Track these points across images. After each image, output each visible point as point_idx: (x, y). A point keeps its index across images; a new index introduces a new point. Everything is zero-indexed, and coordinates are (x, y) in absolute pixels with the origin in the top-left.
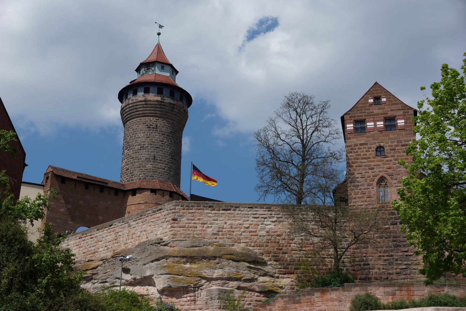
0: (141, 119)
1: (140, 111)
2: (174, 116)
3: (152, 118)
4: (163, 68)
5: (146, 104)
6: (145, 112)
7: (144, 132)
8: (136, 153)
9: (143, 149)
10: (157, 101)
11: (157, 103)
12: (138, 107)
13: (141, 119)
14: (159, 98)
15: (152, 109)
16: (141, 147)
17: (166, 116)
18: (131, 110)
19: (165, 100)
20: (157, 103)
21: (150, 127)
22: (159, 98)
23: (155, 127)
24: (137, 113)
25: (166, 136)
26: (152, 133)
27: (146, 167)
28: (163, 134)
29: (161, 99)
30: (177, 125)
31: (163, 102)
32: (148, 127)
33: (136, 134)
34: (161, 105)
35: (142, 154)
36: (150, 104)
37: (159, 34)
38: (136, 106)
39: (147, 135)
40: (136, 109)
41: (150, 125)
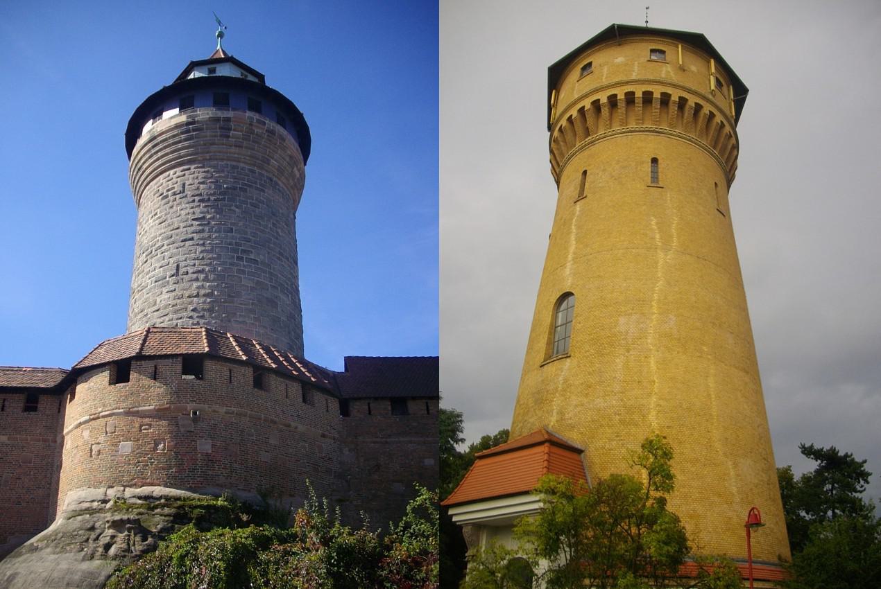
2: (233, 149)
3: (172, 172)
7: (153, 214)
11: (176, 132)
15: (168, 150)
17: (207, 156)
21: (167, 197)
26: (172, 207)
30: (253, 172)
32: (163, 199)
34: (188, 131)
35: (148, 273)
36: (162, 142)
39: (159, 218)
41: (168, 191)
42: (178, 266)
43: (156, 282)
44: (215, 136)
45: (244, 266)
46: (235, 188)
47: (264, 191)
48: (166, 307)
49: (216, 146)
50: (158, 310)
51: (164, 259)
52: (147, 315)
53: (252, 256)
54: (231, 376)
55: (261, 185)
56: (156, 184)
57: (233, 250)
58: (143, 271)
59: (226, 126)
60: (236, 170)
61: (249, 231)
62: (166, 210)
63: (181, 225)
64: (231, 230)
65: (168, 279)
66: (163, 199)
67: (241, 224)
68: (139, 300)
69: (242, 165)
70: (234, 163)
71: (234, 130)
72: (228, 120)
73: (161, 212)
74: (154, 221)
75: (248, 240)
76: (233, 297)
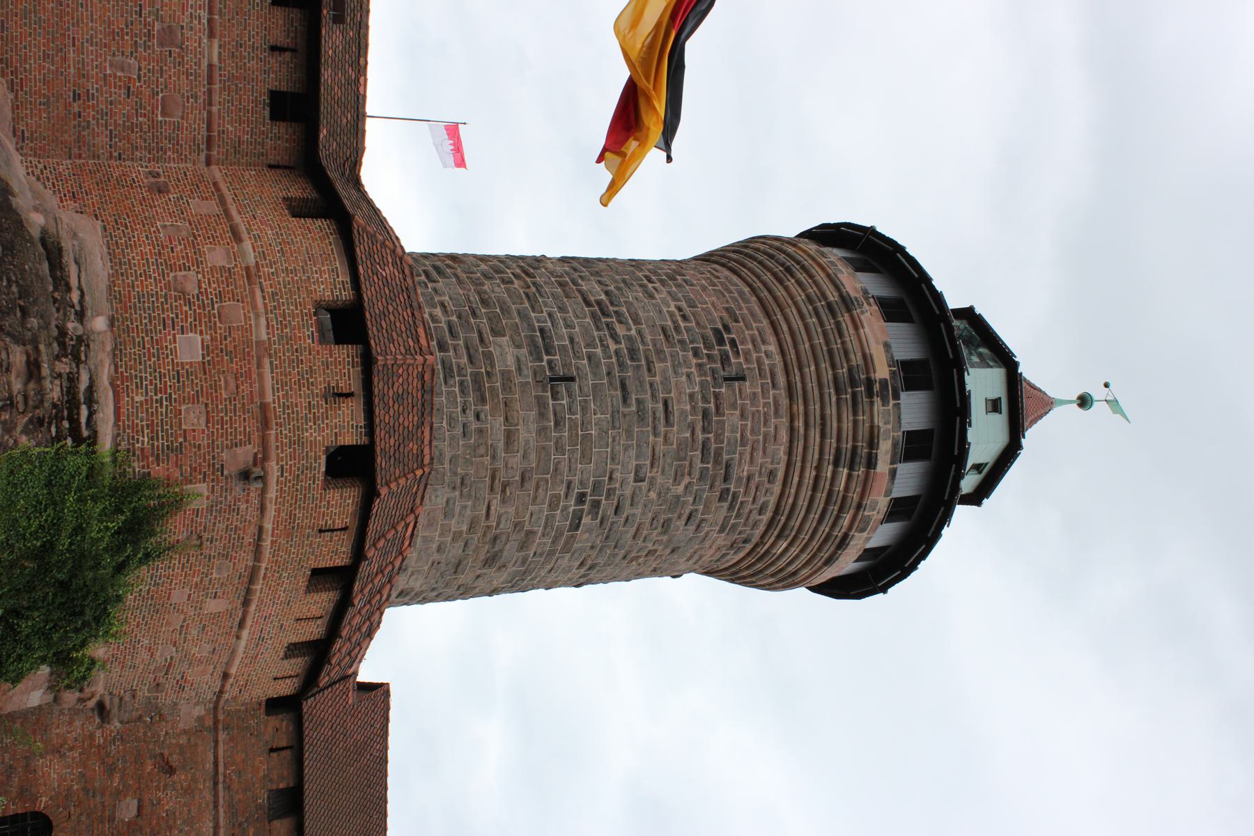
0: (746, 301)
1: (786, 288)
3: (773, 348)
4: (994, 406)
5: (829, 306)
6: (792, 312)
7: (687, 310)
8: (562, 285)
9: (593, 315)
10: (867, 359)
11: (856, 359)
12: (802, 277)
13: (746, 301)
14: (882, 371)
15: (819, 340)
16: (599, 303)
17: (800, 424)
18: (772, 257)
19: (885, 402)
20: (856, 359)
21: (721, 341)
22: (882, 371)
23: (733, 371)
24: (768, 277)
25: (700, 436)
26: (696, 353)
27: (496, 333)
28: (705, 414)
29: (884, 383)
31: (870, 394)
32: (717, 332)
33: (662, 282)
34: (853, 382)
35: (562, 309)
36: (838, 324)
37: (1084, 401)
38: (803, 267)
39: (677, 328)
40: (788, 270)
41: (733, 343)
42: (572, 379)
43: (542, 331)
44: (839, 440)
45: (566, 508)
46: (726, 479)
47: (722, 530)
48: (488, 356)
49: (818, 439)
50: (482, 340)
51: (587, 345)
52: (474, 314)
53: (586, 520)
54: (333, 531)
55: (734, 526)
56: (752, 314)
57: (597, 487)
58: (567, 297)
59: (858, 460)
60: (766, 479)
61: (638, 511)
62: (692, 342)
63: (657, 378)
64: (638, 479)
65: (545, 358)
66: (716, 331)
67: (653, 495)
68: (508, 290)
69: (777, 488)
70: (780, 475)
71: (849, 476)
72: (871, 463)
73: (688, 330)
74: (671, 314)
75: (617, 510)
76: (504, 491)
